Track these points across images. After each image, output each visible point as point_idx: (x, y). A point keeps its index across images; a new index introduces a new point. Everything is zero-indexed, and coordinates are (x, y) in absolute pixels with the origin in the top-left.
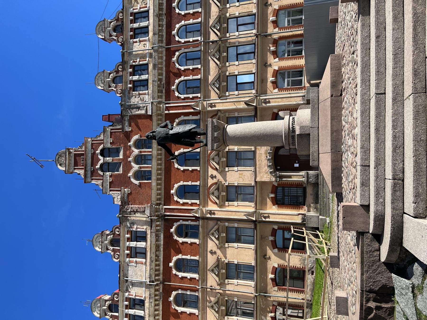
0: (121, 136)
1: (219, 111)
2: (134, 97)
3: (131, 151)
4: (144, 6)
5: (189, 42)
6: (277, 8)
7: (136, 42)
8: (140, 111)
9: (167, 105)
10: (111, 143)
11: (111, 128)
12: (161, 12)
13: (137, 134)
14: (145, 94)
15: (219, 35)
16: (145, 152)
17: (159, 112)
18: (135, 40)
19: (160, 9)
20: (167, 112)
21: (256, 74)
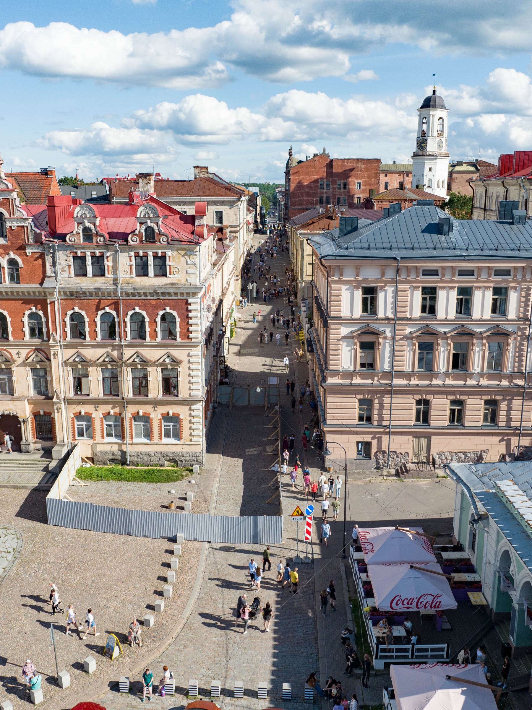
0: (20, 241)
1: (50, 360)
2: (66, 258)
3: (3, 255)
4: (172, 270)
5: (126, 326)
6: (151, 416)
7: (131, 261)
8: (50, 267)
9: (56, 303)
10: (11, 227)
11: (29, 227)
12: (160, 294)
13: (23, 263)
14: (70, 273)
15: (128, 362)
16: (4, 274)
17: (47, 294)
18: (133, 259)
19: (164, 294)
20: (48, 302)
21: (87, 398)
